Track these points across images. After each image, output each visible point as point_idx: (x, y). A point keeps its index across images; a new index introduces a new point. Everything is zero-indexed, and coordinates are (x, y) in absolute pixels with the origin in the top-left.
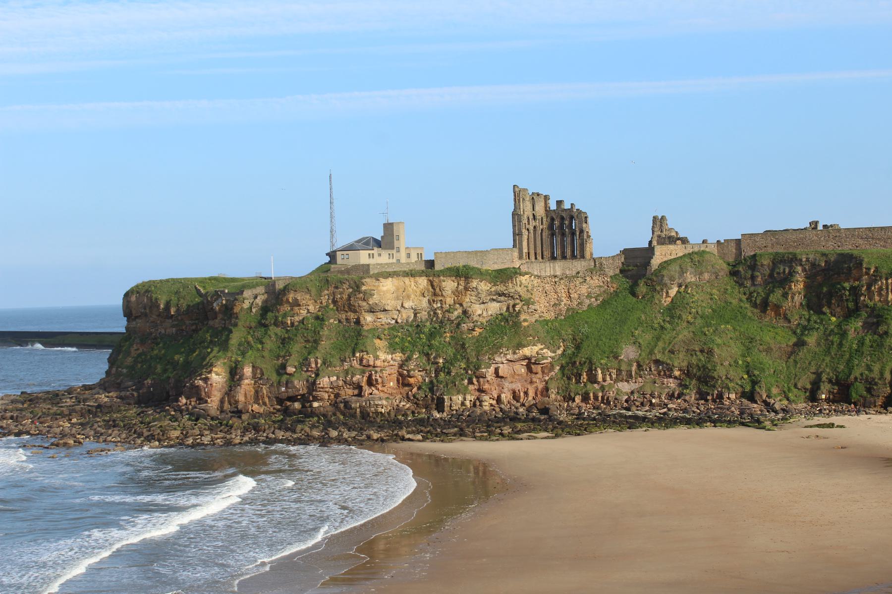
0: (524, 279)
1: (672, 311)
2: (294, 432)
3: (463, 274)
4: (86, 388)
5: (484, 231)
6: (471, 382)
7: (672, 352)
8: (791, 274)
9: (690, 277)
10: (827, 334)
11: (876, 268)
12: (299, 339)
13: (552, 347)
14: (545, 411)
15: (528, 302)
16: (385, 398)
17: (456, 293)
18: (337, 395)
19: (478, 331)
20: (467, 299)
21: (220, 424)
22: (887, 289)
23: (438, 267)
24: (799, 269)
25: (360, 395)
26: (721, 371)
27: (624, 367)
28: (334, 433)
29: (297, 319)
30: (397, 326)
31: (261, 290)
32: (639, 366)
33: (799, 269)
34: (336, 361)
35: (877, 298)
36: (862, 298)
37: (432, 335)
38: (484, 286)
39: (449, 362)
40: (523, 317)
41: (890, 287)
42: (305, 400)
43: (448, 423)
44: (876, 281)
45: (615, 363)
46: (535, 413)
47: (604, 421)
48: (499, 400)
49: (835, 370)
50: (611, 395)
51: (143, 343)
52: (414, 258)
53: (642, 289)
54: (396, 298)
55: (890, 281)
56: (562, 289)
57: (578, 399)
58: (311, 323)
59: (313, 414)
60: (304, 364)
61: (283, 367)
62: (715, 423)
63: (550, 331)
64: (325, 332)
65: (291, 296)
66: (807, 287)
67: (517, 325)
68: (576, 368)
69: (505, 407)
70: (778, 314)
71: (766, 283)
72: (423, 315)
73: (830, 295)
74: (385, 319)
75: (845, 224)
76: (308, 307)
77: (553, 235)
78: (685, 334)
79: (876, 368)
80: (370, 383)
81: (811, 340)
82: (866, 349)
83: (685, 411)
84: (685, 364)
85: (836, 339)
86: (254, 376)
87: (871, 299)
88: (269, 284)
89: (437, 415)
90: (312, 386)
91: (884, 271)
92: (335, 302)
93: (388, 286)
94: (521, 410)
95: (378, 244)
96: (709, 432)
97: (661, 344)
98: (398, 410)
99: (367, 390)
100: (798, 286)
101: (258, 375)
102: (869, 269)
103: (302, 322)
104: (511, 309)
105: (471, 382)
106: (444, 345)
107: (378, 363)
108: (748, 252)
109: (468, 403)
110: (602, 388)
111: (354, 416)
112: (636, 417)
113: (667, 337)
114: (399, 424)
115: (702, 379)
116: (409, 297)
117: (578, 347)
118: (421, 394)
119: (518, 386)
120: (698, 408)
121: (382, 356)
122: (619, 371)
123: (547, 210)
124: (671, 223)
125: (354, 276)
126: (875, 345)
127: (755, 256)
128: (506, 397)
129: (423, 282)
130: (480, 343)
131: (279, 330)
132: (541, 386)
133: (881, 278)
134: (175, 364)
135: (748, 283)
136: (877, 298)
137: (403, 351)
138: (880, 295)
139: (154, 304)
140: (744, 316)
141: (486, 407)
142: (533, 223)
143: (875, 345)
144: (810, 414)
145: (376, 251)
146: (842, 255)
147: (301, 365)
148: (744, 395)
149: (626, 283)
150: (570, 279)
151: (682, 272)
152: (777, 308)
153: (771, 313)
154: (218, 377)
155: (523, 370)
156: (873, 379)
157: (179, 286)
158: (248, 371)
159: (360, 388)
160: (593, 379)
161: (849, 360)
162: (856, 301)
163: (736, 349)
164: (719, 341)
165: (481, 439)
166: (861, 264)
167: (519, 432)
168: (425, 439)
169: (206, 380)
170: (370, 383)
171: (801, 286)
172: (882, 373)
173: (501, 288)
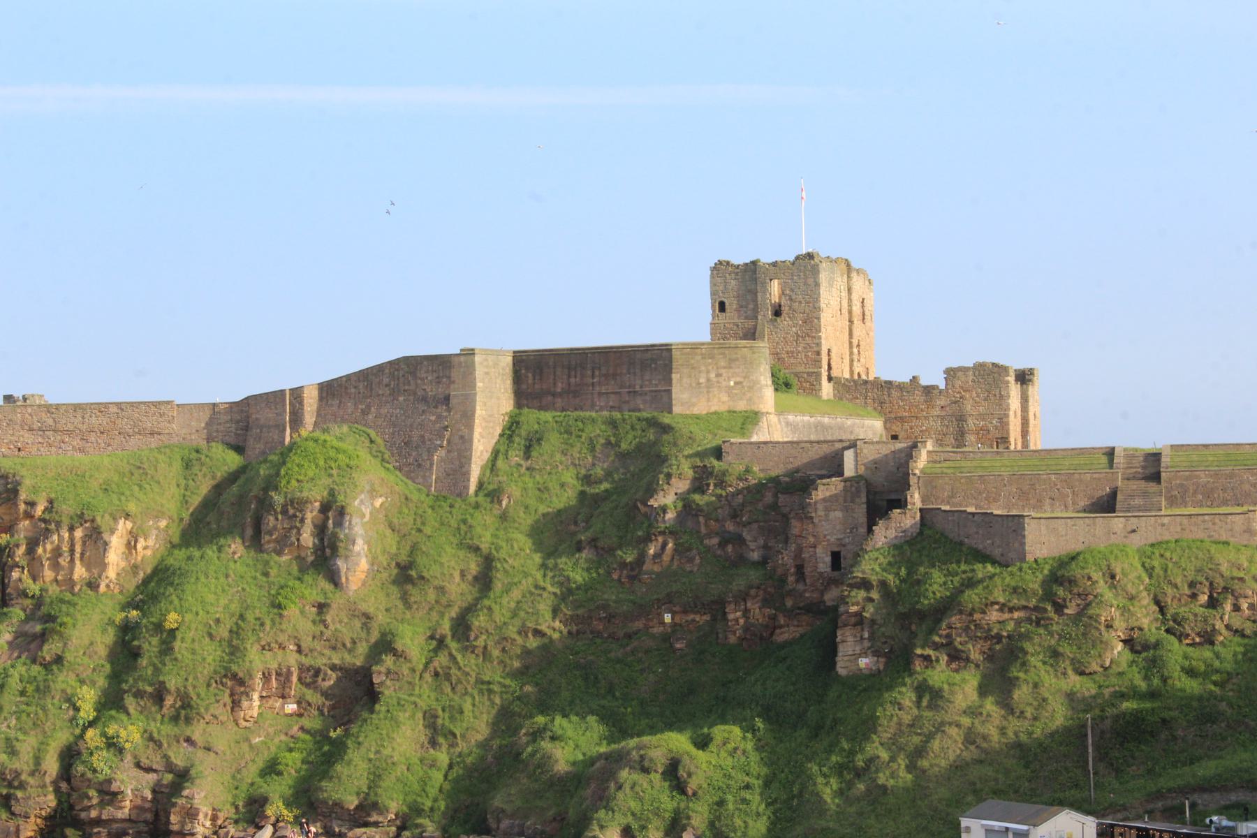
11: (51, 502)
22: (72, 551)
35: (48, 574)
36: (15, 574)
41: (78, 549)
44: (47, 533)
55: (79, 533)
75: (54, 397)
79: (27, 746)
87: (34, 580)
91: (67, 509)
102: (32, 504)
126: (30, 688)
133: (58, 524)
136: (48, 574)
138: (56, 566)
143: (30, 688)
156: (17, 774)
166: (15, 492)
172: (38, 761)
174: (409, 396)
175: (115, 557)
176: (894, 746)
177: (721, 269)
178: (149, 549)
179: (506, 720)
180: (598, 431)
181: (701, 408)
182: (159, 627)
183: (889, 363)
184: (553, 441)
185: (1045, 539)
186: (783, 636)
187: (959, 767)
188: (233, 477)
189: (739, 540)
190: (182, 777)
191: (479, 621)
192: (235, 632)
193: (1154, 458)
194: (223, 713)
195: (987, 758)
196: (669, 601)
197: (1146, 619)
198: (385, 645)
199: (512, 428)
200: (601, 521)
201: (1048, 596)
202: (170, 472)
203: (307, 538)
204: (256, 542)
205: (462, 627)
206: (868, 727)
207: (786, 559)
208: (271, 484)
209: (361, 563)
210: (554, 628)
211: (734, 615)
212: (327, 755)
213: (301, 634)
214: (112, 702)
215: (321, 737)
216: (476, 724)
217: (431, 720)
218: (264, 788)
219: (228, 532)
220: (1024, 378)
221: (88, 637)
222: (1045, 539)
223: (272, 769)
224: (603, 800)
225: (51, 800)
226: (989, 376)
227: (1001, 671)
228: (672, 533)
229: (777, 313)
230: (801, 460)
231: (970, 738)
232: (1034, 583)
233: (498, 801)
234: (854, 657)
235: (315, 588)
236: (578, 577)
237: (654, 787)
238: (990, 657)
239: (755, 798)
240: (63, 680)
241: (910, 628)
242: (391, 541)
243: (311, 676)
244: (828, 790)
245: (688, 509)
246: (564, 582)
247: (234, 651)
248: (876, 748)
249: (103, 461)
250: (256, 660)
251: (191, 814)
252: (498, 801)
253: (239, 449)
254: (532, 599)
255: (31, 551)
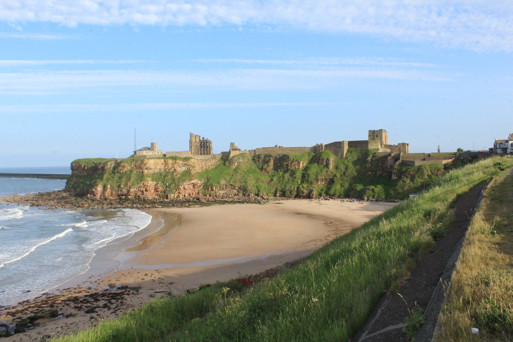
0: (193, 160)
1: (235, 170)
2: (123, 205)
3: (174, 158)
4: (59, 191)
5: (182, 146)
6: (176, 190)
7: (235, 182)
8: (270, 160)
9: (241, 160)
10: (279, 177)
12: (125, 177)
13: (201, 180)
14: (198, 199)
15: (194, 167)
16: (150, 195)
17: (172, 164)
18: (136, 194)
19: (179, 175)
20: (175, 166)
21: (100, 203)
23: (167, 156)
24: (272, 159)
25: (143, 194)
26: (249, 188)
27: (221, 186)
28: (135, 206)
29: (124, 171)
30: (154, 174)
31: (113, 162)
32: (226, 186)
33: (272, 159)
34: (136, 184)
37: (165, 176)
38: (181, 162)
39: (170, 184)
40: (192, 171)
42: (126, 195)
43: (169, 203)
45: (219, 185)
46: (195, 200)
47: (215, 202)
48: (185, 196)
49: (281, 187)
50: (218, 194)
51: (77, 177)
52: (160, 153)
53: (227, 163)
54: (154, 166)
56: (204, 163)
57: (208, 196)
58: (128, 172)
59: (128, 200)
60: (126, 185)
61: (120, 185)
62: (247, 202)
63: (200, 176)
64: (133, 175)
65: (122, 164)
66: (274, 164)
67: (190, 174)
68: (207, 186)
69: (186, 198)
70: (266, 171)
71: (262, 162)
72: (162, 171)
73: (280, 166)
74: (151, 172)
75: (285, 146)
76: (127, 168)
77: (201, 147)
78: (239, 177)
80: (146, 190)
81: (275, 179)
82: (290, 182)
83: (239, 199)
84: (239, 186)
85: (282, 179)
86: (111, 188)
88: (116, 161)
89: (166, 200)
90: (128, 191)
91: (295, 160)
92: (136, 166)
93: (152, 161)
94: (191, 199)
95: (149, 149)
96: (246, 205)
97: (232, 180)
98: (154, 199)
99: (145, 193)
100: (271, 163)
101: (112, 188)
103: (126, 172)
104: (188, 169)
105: (176, 190)
106: (169, 180)
107: (149, 185)
108: (257, 153)
109: (175, 197)
110: (215, 192)
111: (141, 200)
112: (225, 201)
113: (234, 178)
114: (155, 203)
115: (244, 190)
116: (158, 165)
117: (208, 180)
118: (161, 194)
119: (190, 192)
120: (242, 198)
121: (150, 182)
122: (220, 187)
123: (200, 140)
124: (236, 145)
125: (142, 159)
127: (259, 155)
128: (187, 195)
129: (162, 161)
130: (179, 179)
131: (118, 175)
132: (197, 192)
134: (86, 185)
135: (257, 162)
137: (156, 181)
139: (80, 166)
140: (256, 172)
141: (181, 198)
142: (195, 144)
144: (274, 200)
145: (148, 151)
146: (284, 155)
147: (125, 185)
148: (256, 195)
149: (222, 162)
150: (206, 160)
151: (239, 159)
152: (265, 170)
153: (264, 171)
154: (100, 188)
155: (192, 187)
157: (88, 160)
158: (109, 186)
159: (143, 192)
160: (212, 190)
161: (285, 185)
162: (287, 168)
163: (254, 181)
164: (249, 179)
165: (179, 207)
167: (191, 205)
168: (162, 207)
169: (96, 189)
170: (146, 190)
171: (272, 163)
173: (185, 163)
174: (336, 146)
175: (301, 165)
176: (400, 187)
177: (370, 131)
178: (305, 164)
179: (350, 185)
180: (359, 151)
181: (372, 148)
182: (307, 173)
183: (389, 143)
184: (354, 152)
185: (417, 163)
186: (384, 175)
187: (408, 190)
188: (314, 156)
189: (378, 164)
190: (312, 191)
191: (346, 173)
192: (317, 174)
193: (429, 154)
194: (316, 183)
195: (411, 189)
196: (370, 171)
197: (429, 173)
198: (335, 176)
199: (348, 150)
200: (361, 161)
201: (418, 170)
202: (307, 155)
203: (325, 163)
204: (318, 164)
205: (344, 174)
206: (397, 185)
207: (384, 166)
208: (320, 157)
209: (331, 166)
210: (356, 174)
211: (378, 172)
212: (329, 188)
213: (324, 174)
214: (302, 182)
215: (328, 186)
216: (347, 185)
217: (341, 184)
218: (321, 192)
219: (315, 162)
220: (408, 144)
221: (299, 174)
222: (417, 163)
223: (322, 190)
224: (365, 193)
225: (296, 193)
226: (404, 145)
227: (412, 178)
228: (370, 163)
229: (377, 136)
230: (385, 154)
231: (409, 186)
232: (416, 169)
233: (351, 194)
234: (394, 177)
235: (326, 169)
236: (358, 168)
237: (371, 192)
238: (411, 177)
239: (383, 194)
240: (296, 179)
241: (401, 174)
242: (335, 164)
243: (326, 179)
244: (392, 192)
245: (372, 160)
246: (357, 169)
247: (317, 176)
248: (398, 187)
249: (299, 154)
250: (320, 178)
251: (313, 195)
252: (351, 194)
253: (315, 153)
254: (352, 171)
255: (291, 164)
